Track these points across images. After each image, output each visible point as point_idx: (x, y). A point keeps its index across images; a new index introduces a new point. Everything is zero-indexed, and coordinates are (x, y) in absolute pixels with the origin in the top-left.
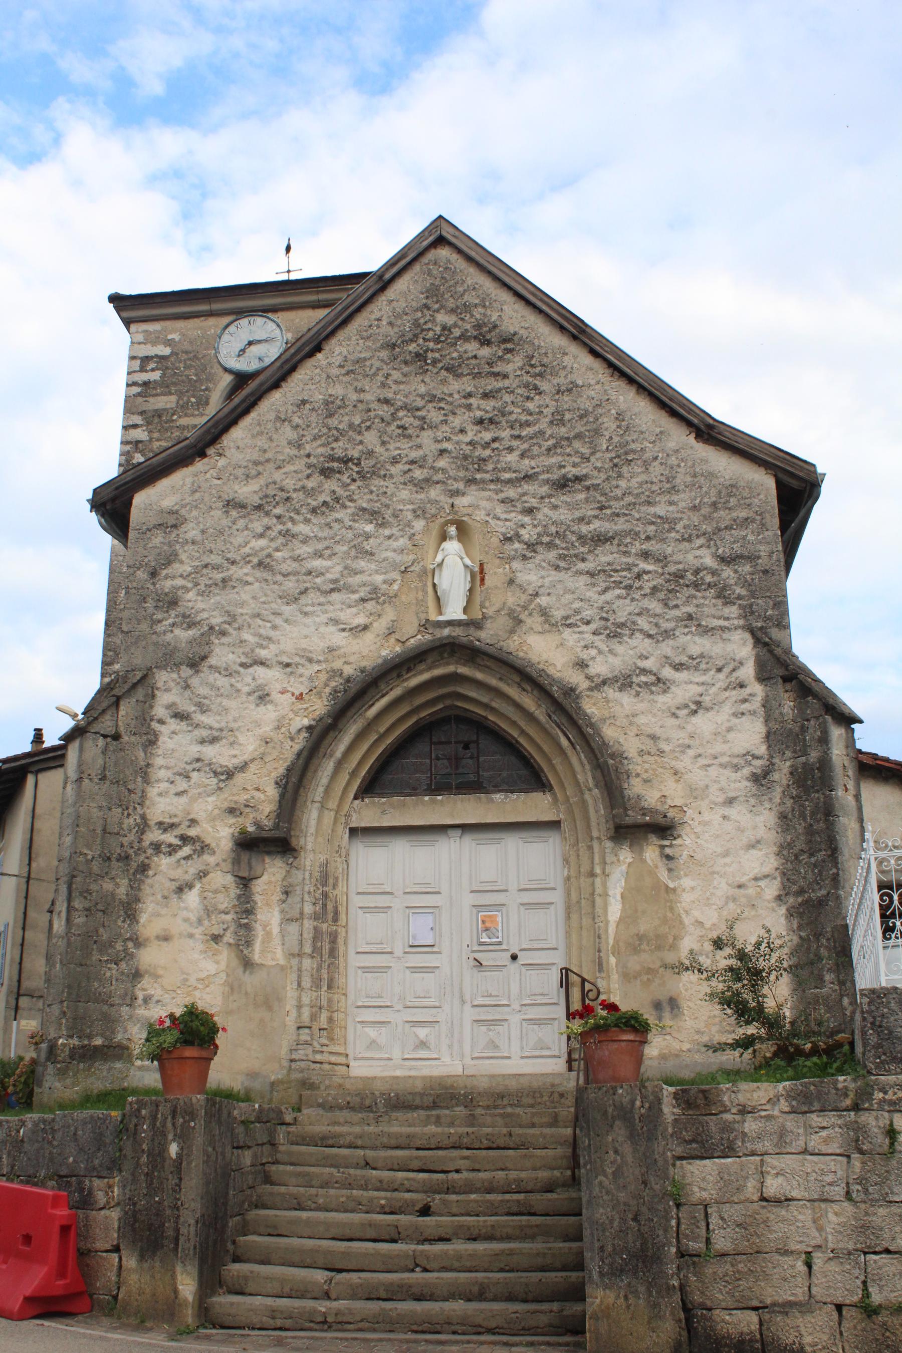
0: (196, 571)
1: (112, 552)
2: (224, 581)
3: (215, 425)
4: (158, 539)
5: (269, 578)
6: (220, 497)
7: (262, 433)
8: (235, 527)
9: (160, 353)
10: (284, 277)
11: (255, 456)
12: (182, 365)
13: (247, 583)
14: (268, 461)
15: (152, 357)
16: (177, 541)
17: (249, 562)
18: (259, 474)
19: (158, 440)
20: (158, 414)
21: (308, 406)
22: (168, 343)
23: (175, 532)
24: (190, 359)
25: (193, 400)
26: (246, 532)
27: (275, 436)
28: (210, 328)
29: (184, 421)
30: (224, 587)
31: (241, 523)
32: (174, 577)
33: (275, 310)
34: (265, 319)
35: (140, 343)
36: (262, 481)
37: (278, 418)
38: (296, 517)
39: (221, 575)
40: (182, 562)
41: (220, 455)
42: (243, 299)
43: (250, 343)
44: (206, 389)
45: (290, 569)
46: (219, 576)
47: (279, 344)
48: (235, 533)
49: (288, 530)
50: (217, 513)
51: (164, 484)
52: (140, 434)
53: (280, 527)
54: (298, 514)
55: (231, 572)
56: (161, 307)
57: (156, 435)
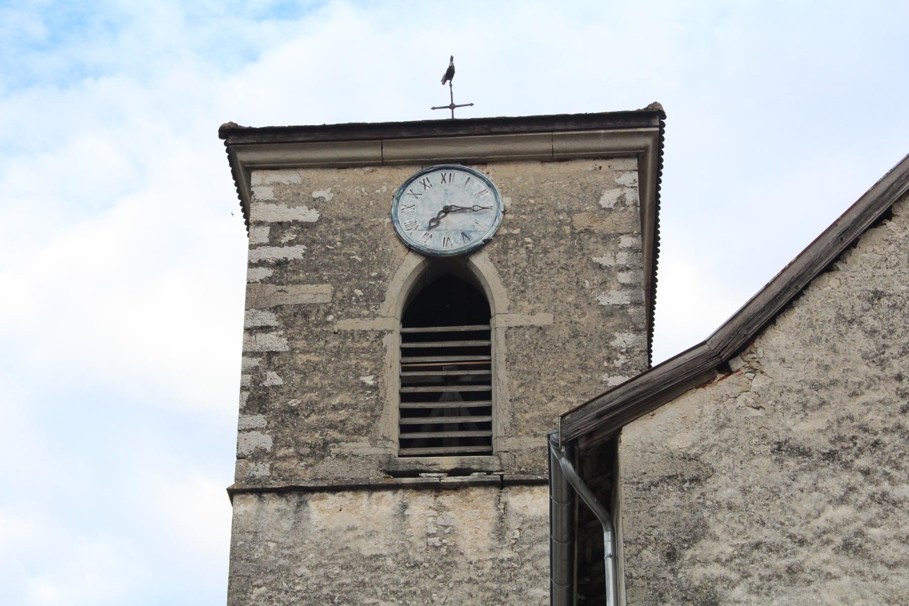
0: (742, 553)
1: (234, 527)
2: (790, 570)
3: (747, 323)
4: (670, 500)
5: (866, 569)
6: (764, 437)
7: (819, 340)
8: (795, 485)
9: (301, 219)
10: (445, 115)
11: (813, 375)
12: (338, 238)
13: (829, 576)
14: (834, 383)
15: (289, 224)
16: (703, 504)
17: (828, 542)
18: (823, 403)
19: (304, 352)
20: (303, 311)
21: (884, 301)
22: (315, 203)
23: (698, 491)
24: (350, 230)
25: (359, 292)
26: (816, 494)
27: (839, 345)
28: (381, 183)
29: (346, 325)
30: (793, 582)
31: (805, 480)
32: (706, 563)
33: (483, 161)
34: (467, 175)
35: (267, 202)
36: (829, 414)
37: (840, 317)
38: (894, 473)
39: (785, 562)
40: (716, 539)
41: (754, 371)
42: (434, 143)
43: (447, 210)
44: (379, 277)
45: (897, 557)
46: (782, 564)
47: (492, 213)
48: (799, 494)
49: (884, 494)
50: (766, 462)
51: (669, 413)
52: (274, 342)
53: (871, 488)
54: (898, 468)
55: (800, 557)
56: (304, 148)
57: (301, 344)
